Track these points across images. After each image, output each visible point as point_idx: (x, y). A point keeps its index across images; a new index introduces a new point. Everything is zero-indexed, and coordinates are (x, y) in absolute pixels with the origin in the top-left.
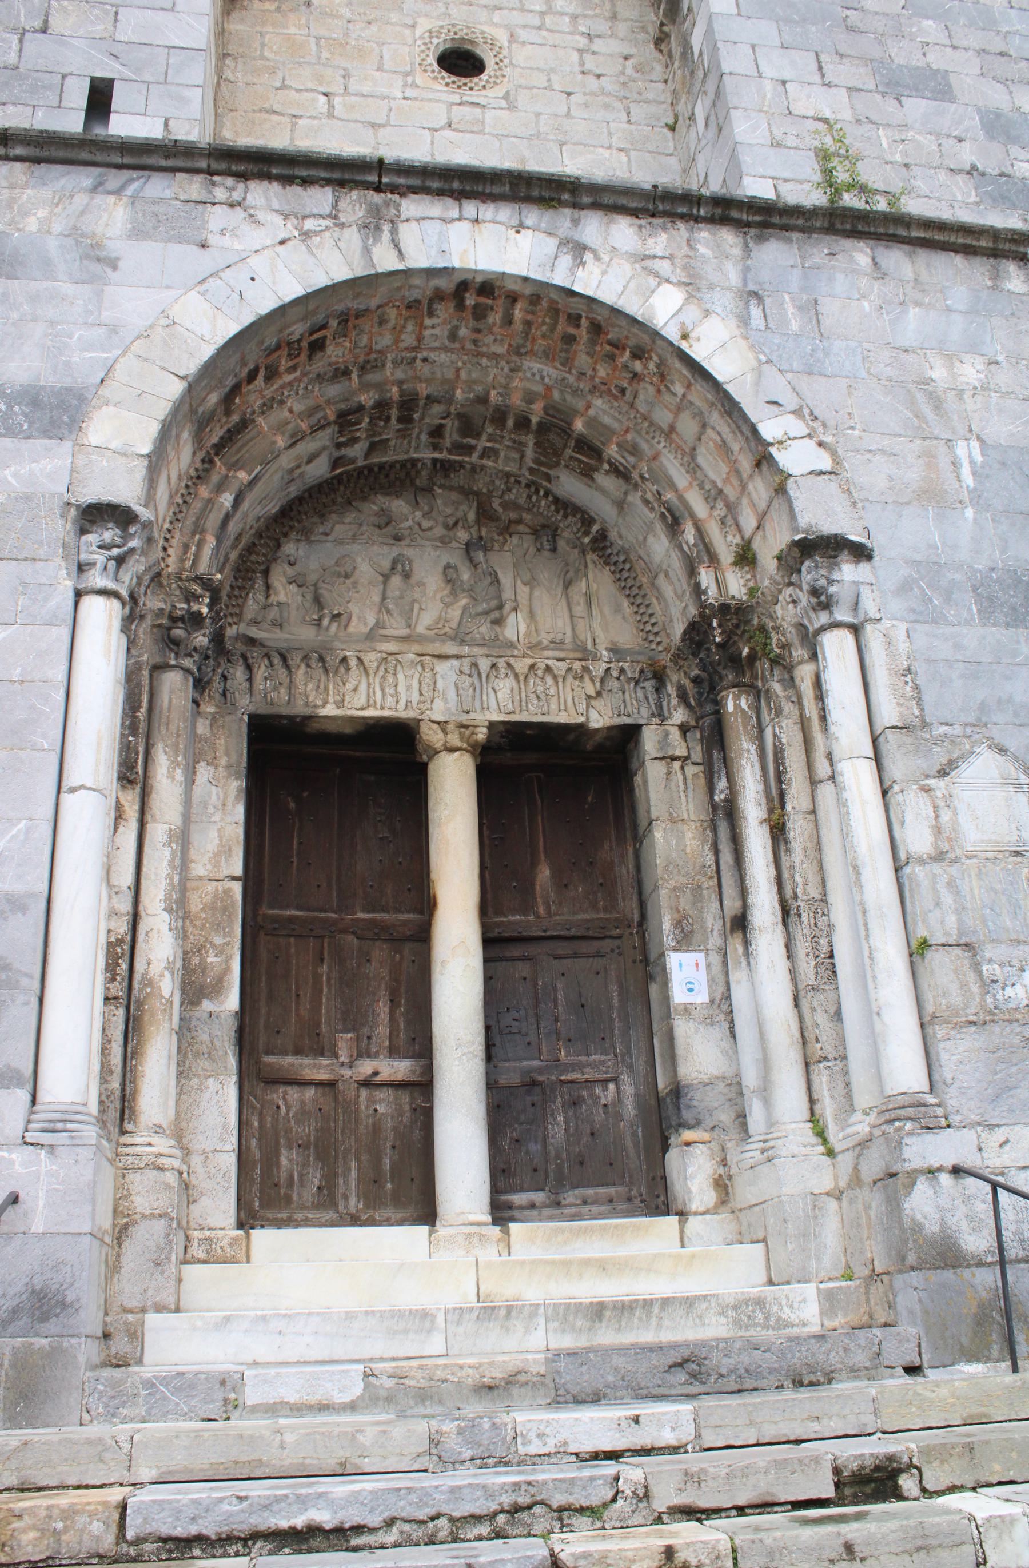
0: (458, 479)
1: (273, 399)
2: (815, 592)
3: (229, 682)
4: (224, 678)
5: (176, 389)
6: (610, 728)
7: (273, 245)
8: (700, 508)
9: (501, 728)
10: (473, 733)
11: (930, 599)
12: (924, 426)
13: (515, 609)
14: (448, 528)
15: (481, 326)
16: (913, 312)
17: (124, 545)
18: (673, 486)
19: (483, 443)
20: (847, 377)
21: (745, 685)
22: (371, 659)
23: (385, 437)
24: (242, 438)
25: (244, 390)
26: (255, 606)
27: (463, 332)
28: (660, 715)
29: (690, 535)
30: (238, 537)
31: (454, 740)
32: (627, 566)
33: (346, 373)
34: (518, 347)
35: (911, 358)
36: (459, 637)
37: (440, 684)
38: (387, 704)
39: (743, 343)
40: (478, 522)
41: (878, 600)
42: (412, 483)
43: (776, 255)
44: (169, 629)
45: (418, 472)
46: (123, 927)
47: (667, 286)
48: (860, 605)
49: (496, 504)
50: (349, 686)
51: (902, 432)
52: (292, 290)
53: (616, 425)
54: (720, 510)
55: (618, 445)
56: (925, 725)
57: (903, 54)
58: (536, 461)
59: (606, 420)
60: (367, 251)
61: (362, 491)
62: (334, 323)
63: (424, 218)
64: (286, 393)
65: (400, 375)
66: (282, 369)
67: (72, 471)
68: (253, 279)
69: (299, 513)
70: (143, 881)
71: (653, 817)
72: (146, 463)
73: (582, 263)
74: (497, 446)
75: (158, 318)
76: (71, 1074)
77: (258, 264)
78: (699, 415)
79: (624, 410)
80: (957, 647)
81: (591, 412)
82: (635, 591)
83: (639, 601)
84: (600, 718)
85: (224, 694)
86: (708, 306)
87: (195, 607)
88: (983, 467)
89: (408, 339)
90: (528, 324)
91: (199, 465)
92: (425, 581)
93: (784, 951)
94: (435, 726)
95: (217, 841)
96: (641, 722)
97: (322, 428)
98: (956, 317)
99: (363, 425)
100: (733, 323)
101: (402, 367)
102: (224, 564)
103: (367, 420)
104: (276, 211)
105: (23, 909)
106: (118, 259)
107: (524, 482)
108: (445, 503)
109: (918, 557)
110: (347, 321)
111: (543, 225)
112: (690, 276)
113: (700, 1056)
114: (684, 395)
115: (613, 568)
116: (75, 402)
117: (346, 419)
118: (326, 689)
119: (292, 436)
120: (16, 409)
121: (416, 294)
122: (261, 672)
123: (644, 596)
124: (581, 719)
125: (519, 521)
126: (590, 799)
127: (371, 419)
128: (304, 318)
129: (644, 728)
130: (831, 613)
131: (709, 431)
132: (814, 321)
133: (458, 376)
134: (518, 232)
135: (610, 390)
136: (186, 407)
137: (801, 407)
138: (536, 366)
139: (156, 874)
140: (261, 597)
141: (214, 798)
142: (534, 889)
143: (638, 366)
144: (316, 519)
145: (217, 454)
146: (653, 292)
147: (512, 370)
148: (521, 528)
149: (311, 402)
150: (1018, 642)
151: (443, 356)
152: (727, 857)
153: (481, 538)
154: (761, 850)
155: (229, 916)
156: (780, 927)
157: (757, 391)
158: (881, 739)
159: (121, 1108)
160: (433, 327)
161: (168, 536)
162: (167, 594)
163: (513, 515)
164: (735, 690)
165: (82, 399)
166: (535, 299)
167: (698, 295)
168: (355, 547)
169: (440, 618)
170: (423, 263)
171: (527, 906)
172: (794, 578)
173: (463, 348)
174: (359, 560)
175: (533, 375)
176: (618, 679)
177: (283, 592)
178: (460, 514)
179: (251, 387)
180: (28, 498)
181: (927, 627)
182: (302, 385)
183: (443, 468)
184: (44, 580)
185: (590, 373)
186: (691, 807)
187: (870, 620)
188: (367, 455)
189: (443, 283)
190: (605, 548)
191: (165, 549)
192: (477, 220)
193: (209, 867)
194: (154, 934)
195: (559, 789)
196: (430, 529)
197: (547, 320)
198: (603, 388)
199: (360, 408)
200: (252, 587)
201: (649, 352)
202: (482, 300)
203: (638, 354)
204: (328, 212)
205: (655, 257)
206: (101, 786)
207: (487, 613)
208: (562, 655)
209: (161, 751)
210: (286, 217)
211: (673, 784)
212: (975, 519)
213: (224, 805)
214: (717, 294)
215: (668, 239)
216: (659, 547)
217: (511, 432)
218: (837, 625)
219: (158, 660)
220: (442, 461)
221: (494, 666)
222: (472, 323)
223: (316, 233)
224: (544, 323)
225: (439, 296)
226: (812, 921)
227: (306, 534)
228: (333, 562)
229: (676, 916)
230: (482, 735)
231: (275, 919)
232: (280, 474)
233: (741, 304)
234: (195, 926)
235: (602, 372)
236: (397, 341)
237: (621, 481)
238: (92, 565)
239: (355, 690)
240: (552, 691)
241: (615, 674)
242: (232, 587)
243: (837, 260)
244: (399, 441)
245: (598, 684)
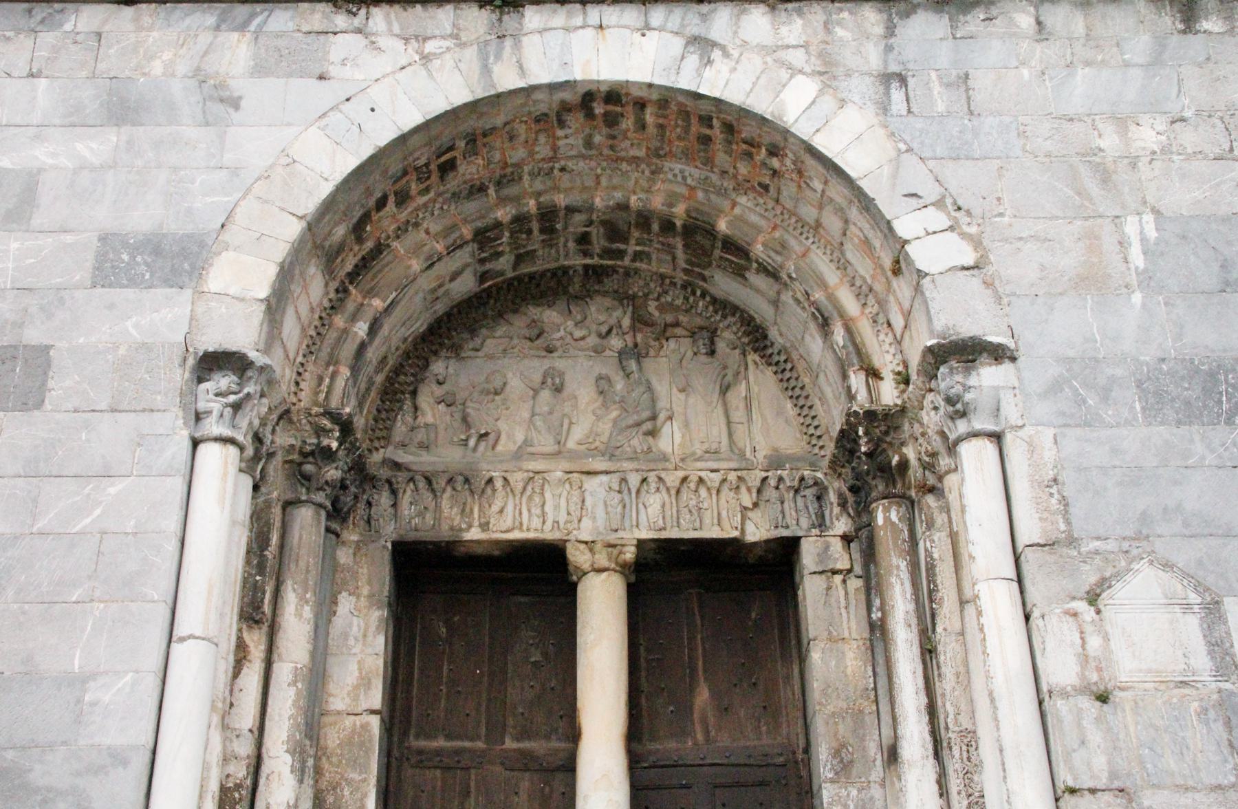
0: (610, 284)
1: (408, 222)
2: (950, 401)
3: (373, 509)
4: (369, 504)
5: (294, 229)
6: (767, 541)
7: (394, 72)
8: (851, 305)
9: (653, 545)
10: (620, 553)
11: (1084, 401)
12: (1087, 203)
13: (670, 418)
14: (600, 336)
15: (616, 133)
16: (1082, 73)
17: (239, 392)
18: (823, 285)
19: (632, 248)
20: (998, 158)
21: (895, 496)
22: (517, 479)
23: (530, 248)
24: (376, 265)
25: (375, 217)
26: (404, 428)
27: (597, 139)
28: (821, 523)
29: (839, 336)
30: (383, 361)
31: (602, 560)
32: (789, 366)
33: (482, 189)
34: (657, 149)
35: (1077, 127)
36: (611, 453)
37: (588, 503)
38: (533, 526)
39: (881, 132)
40: (633, 328)
41: (1021, 404)
42: (566, 292)
44: (300, 464)
45: (570, 279)
46: (240, 771)
47: (800, 77)
48: (1002, 410)
49: (652, 306)
50: (495, 508)
51: (1060, 214)
52: (412, 118)
53: (763, 223)
54: (872, 308)
55: (764, 245)
56: (1072, 541)
58: (688, 262)
59: (754, 218)
60: (486, 70)
61: (513, 303)
62: (461, 144)
63: (546, 30)
64: (421, 215)
65: (538, 185)
66: (413, 192)
67: (191, 319)
68: (373, 110)
69: (449, 329)
70: (267, 723)
71: (811, 636)
72: (263, 307)
73: (710, 62)
74: (646, 249)
75: (278, 157)
77: (378, 94)
78: (840, 211)
79: (770, 207)
80: (1115, 451)
81: (737, 211)
82: (797, 392)
83: (801, 402)
84: (757, 531)
85: (369, 522)
86: (843, 96)
87: (325, 442)
88: (1157, 244)
89: (543, 150)
90: (661, 127)
91: (332, 295)
92: (577, 393)
93: (936, 788)
94: (582, 546)
95: (356, 674)
96: (800, 534)
97: (460, 247)
98: (1135, 73)
99: (504, 239)
100: (871, 110)
101: (540, 178)
102: (368, 390)
103: (507, 234)
104: (397, 36)
105: (125, 763)
106: (240, 98)
107: (679, 283)
108: (600, 311)
109: (1071, 353)
110: (475, 141)
111: (669, 25)
112: (826, 63)
114: (823, 191)
115: (774, 368)
116: (195, 249)
117: (484, 237)
118: (472, 511)
119: (427, 259)
120: (139, 259)
121: (543, 108)
122: (406, 499)
123: (807, 397)
124: (735, 534)
125: (677, 324)
126: (753, 615)
127: (512, 234)
128: (429, 144)
129: (803, 541)
130: (969, 421)
131: (852, 227)
132: (964, 101)
133: (598, 183)
134: (643, 35)
135: (753, 187)
136: (309, 245)
137: (944, 197)
138: (678, 167)
139: (280, 715)
140: (409, 419)
141: (355, 629)
142: (692, 714)
143: (775, 163)
144: (466, 335)
145: (351, 283)
146: (784, 86)
147: (653, 173)
148: (678, 331)
149: (447, 222)
150: (1192, 441)
151: (581, 164)
152: (882, 682)
153: (636, 345)
154: (910, 676)
155: (366, 752)
156: (931, 760)
157: (894, 185)
158: (1022, 558)
160: (566, 137)
161: (301, 370)
162: (298, 430)
163: (669, 318)
164: (885, 501)
165: (202, 245)
166: (663, 103)
167: (835, 84)
168: (506, 360)
169: (591, 432)
170: (545, 79)
171: (683, 732)
172: (933, 384)
173: (601, 154)
174: (510, 375)
175: (675, 175)
176: (777, 488)
177: (430, 410)
178: (613, 321)
179: (381, 214)
180: (145, 347)
181: (1078, 431)
182: (438, 206)
183: (595, 274)
184: (161, 431)
185: (732, 171)
186: (853, 625)
187: (1012, 427)
188: (515, 268)
189: (567, 96)
190: (765, 347)
191: (297, 384)
192: (601, 27)
193: (347, 700)
194: (274, 777)
196: (583, 338)
197: (680, 122)
198: (748, 185)
199: (498, 225)
200: (401, 409)
201: (783, 149)
202: (610, 108)
203: (774, 151)
204: (449, 32)
205: (788, 47)
206: (211, 634)
207: (638, 424)
208: (714, 465)
209: (290, 588)
210: (407, 40)
211: (833, 600)
212: (1144, 305)
213: (365, 636)
214: (855, 81)
215: (804, 25)
216: (814, 345)
217: (658, 235)
218: (976, 435)
219: (290, 496)
220: (594, 267)
221: (644, 480)
222: (605, 130)
223: (436, 55)
224: (677, 126)
225: (565, 108)
226: (965, 755)
227: (456, 350)
228: (483, 379)
229: (835, 744)
230: (630, 554)
231: (420, 752)
232: (421, 295)
233: (881, 89)
234: (331, 763)
235: (743, 169)
236: (532, 154)
237: (771, 280)
238: (209, 413)
239: (501, 511)
240: (705, 505)
241: (773, 482)
242: (379, 411)
243: (994, 25)
244: (547, 250)
245: (754, 495)
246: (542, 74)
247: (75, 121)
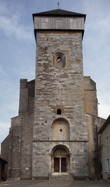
43: (71, 143)
57: (77, 132)
76: (50, 169)
113: (67, 168)
159: (51, 169)
195: (64, 160)
246: (59, 144)
247: (45, 146)
